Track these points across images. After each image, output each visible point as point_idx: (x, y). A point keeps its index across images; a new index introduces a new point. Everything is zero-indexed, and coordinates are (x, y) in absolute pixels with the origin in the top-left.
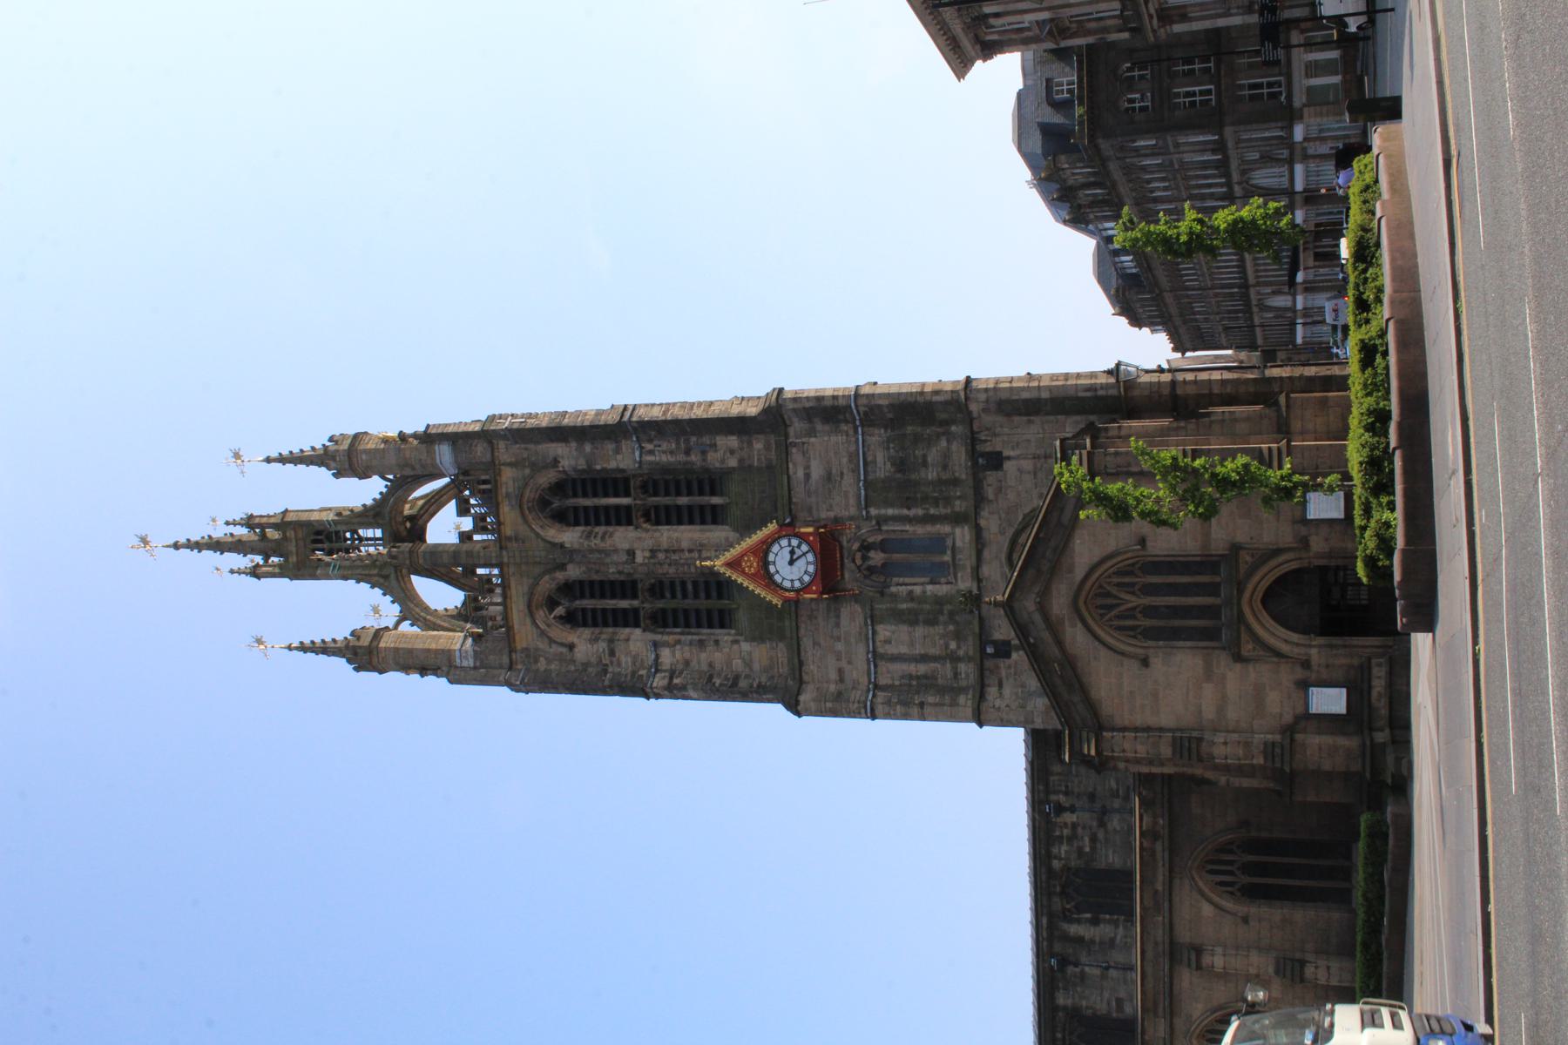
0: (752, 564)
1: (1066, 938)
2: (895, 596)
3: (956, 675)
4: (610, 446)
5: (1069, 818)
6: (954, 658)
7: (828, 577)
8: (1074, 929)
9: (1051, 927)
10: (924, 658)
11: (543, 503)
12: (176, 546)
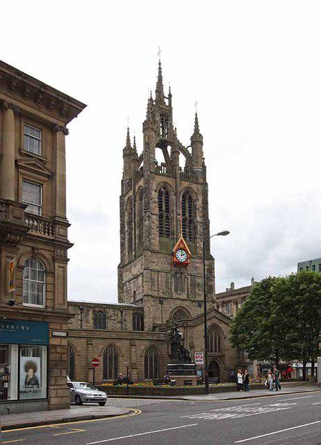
0: (182, 246)
1: (88, 310)
2: (171, 279)
3: (155, 291)
4: (201, 215)
5: (120, 314)
6: (158, 291)
7: (179, 265)
8: (91, 313)
9: (92, 307)
10: (158, 283)
11: (187, 193)
12: (160, 64)
